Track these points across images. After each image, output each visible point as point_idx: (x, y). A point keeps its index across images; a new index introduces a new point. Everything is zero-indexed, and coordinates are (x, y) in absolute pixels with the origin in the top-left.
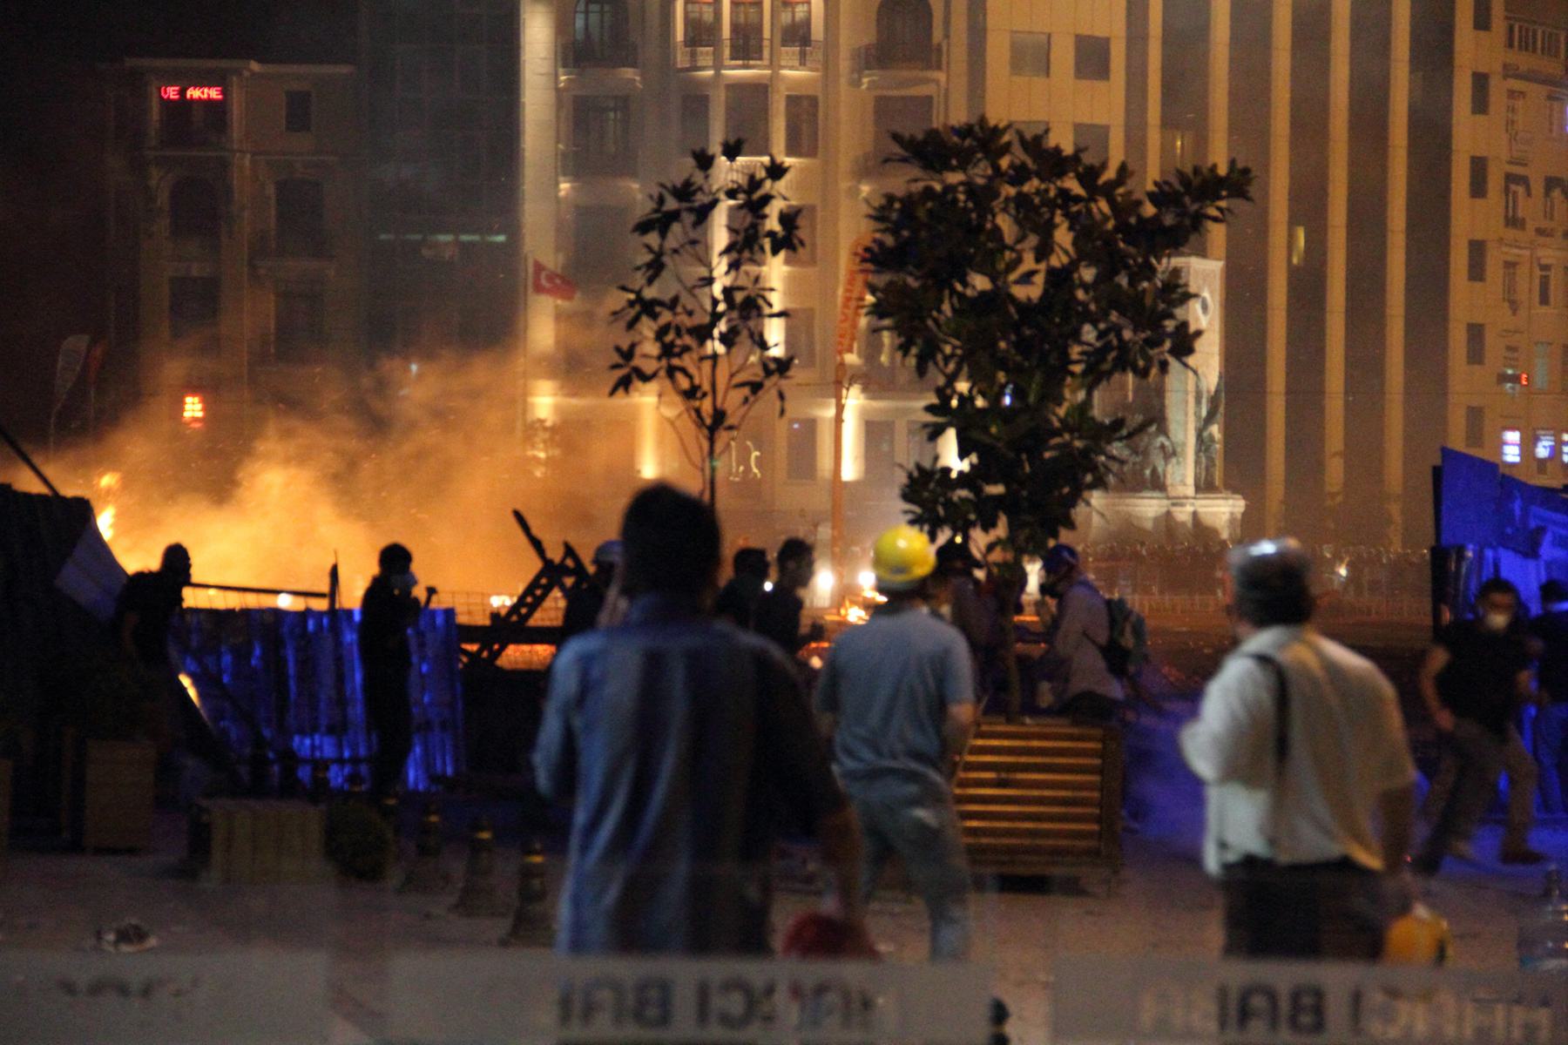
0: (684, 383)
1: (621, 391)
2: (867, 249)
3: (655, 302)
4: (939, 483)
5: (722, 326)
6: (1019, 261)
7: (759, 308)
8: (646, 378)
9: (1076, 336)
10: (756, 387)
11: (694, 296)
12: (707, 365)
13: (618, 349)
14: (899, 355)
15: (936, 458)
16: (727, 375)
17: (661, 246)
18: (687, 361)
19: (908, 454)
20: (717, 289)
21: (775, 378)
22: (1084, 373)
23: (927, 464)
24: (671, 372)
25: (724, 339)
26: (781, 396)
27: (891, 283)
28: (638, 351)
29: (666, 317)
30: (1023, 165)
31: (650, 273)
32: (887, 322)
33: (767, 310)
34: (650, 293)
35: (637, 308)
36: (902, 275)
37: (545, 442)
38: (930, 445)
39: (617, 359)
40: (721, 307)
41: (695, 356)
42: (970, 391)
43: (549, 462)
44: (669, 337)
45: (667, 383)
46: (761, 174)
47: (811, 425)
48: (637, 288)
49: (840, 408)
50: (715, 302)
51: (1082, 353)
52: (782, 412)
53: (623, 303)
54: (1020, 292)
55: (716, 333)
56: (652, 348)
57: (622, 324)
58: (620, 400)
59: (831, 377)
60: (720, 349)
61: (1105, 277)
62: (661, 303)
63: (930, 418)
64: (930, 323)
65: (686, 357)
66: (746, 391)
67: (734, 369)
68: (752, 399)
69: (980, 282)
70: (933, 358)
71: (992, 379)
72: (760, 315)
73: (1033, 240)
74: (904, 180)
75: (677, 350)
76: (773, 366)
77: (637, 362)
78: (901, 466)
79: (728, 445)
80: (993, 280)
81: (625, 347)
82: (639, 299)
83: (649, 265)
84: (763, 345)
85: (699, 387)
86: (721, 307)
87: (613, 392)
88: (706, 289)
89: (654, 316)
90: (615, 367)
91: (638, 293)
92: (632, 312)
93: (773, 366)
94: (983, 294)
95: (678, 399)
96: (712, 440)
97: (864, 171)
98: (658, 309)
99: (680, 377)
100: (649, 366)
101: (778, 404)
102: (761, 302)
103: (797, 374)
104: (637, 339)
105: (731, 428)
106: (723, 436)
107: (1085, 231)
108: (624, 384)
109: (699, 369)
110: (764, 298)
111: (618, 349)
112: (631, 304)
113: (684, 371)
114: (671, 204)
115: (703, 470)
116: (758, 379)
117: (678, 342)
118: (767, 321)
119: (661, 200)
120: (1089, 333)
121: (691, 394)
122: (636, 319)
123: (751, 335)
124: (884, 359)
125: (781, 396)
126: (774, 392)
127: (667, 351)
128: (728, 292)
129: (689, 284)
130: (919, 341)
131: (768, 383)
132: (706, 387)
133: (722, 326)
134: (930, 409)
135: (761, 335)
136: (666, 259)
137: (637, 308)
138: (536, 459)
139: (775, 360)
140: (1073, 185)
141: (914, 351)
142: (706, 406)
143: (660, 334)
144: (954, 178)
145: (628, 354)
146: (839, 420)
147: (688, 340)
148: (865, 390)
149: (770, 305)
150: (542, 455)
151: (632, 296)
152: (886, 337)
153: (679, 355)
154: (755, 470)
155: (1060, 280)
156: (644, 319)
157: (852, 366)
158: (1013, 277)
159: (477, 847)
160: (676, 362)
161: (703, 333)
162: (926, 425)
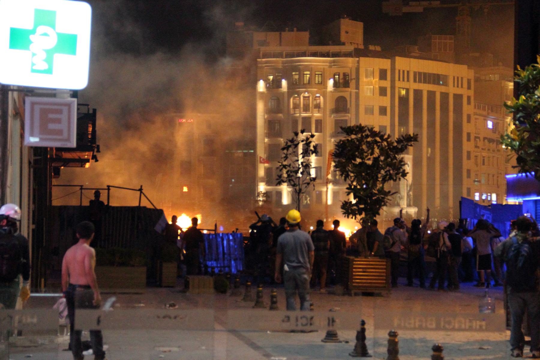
5: (301, 170)
9: (379, 173)
10: (308, 184)
15: (349, 200)
18: (293, 178)
20: (300, 162)
23: (347, 201)
25: (302, 173)
26: (314, 186)
32: (338, 169)
40: (300, 166)
43: (263, 201)
44: (289, 173)
46: (309, 137)
49: (327, 188)
50: (299, 165)
55: (299, 172)
56: (285, 175)
58: (279, 187)
61: (385, 159)
63: (347, 191)
66: (306, 185)
69: (358, 160)
71: (362, 182)
72: (309, 168)
77: (282, 178)
83: (284, 157)
84: (310, 175)
96: (299, 195)
97: (332, 136)
100: (285, 180)
103: (317, 181)
105: (303, 193)
106: (301, 195)
107: (382, 150)
108: (279, 183)
113: (292, 180)
121: (294, 185)
124: (337, 177)
125: (314, 186)
127: (289, 176)
128: (302, 163)
131: (311, 183)
132: (297, 184)
133: (301, 170)
134: (347, 188)
135: (310, 172)
136: (288, 156)
138: (260, 200)
139: (313, 178)
140: (378, 139)
141: (344, 175)
142: (297, 188)
147: (294, 174)
148: (333, 184)
152: (338, 173)
156: (284, 169)
159: (247, 286)
161: (297, 172)
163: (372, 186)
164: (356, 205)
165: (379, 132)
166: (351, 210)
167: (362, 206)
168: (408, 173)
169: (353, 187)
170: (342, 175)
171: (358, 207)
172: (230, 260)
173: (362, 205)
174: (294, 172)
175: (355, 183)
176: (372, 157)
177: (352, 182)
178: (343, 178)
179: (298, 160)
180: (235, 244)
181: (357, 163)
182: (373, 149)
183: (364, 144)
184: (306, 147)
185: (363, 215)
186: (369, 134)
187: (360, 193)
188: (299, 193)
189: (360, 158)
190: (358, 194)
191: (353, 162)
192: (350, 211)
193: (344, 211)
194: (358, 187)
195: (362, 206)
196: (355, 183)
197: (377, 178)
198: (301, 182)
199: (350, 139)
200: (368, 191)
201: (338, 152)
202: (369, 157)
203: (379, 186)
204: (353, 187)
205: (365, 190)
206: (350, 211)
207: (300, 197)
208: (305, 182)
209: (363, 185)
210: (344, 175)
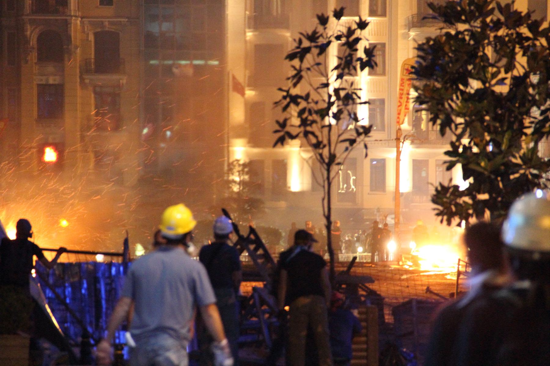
0: (314, 141)
1: (279, 144)
2: (413, 67)
3: (297, 97)
4: (453, 194)
5: (334, 109)
6: (499, 72)
7: (353, 99)
8: (293, 137)
9: (528, 113)
11: (319, 93)
12: (326, 130)
13: (278, 122)
14: (431, 124)
15: (451, 180)
16: (337, 136)
17: (300, 67)
18: (314, 128)
19: (436, 177)
20: (331, 90)
21: (362, 137)
22: (533, 134)
23: (446, 184)
25: (336, 116)
26: (366, 147)
27: (426, 86)
28: (288, 123)
29: (303, 104)
30: (499, 20)
31: (295, 81)
32: (424, 106)
33: (358, 101)
34: (294, 92)
35: (288, 100)
36: (432, 81)
37: (239, 171)
38: (449, 172)
39: (277, 127)
40: (333, 99)
41: (319, 125)
42: (470, 143)
44: (304, 116)
45: (304, 140)
46: (354, 26)
49: (399, 153)
51: (532, 123)
52: (366, 155)
53: (280, 97)
54: (498, 89)
55: (331, 114)
56: (296, 121)
57: (280, 108)
58: (280, 150)
59: (394, 136)
60: (333, 122)
62: (301, 97)
63: (448, 158)
64: (447, 106)
65: (314, 125)
66: (347, 144)
67: (341, 132)
68: (350, 148)
69: (475, 85)
72: (354, 103)
73: (504, 61)
74: (435, 30)
75: (309, 122)
76: (361, 130)
78: (432, 184)
79: (338, 173)
81: (281, 121)
82: (288, 95)
83: (294, 77)
84: (356, 119)
85: (322, 142)
87: (275, 145)
88: (326, 89)
89: (297, 104)
90: (276, 132)
91: (288, 92)
92: (285, 102)
93: (361, 130)
94: (477, 91)
95: (310, 148)
96: (329, 171)
98: (299, 100)
99: (311, 137)
100: (294, 131)
101: (364, 150)
102: (354, 96)
104: (288, 116)
105: (339, 164)
106: (334, 168)
108: (281, 141)
109: (322, 132)
110: (356, 94)
111: (278, 122)
112: (285, 98)
113: (313, 133)
114: (306, 44)
115: (324, 187)
116: (353, 138)
117: (310, 118)
118: (359, 106)
119: (300, 42)
120: (535, 112)
121: (317, 146)
122: (287, 106)
123: (350, 115)
124: (423, 126)
125: (366, 147)
126: (362, 145)
127: (304, 123)
128: (337, 91)
131: (358, 140)
132: (325, 142)
133: (334, 109)
134: (447, 153)
135: (355, 114)
136: (303, 73)
137: (288, 100)
139: (363, 127)
140: (525, 31)
141: (439, 122)
142: (326, 152)
143: (301, 113)
144: (462, 27)
145: (283, 125)
146: (398, 159)
147: (315, 117)
148: (412, 142)
149: (359, 98)
150: (237, 179)
151: (285, 94)
152: (424, 115)
153: (311, 125)
154: (353, 187)
155: (519, 83)
156: (292, 106)
158: (494, 82)
160: (309, 128)
161: (324, 113)
162: (445, 162)
163: (510, 146)
164: (469, 192)
165: (528, 15)
166: (457, 205)
167: (484, 197)
169: (461, 150)
170: (433, 121)
171: (474, 198)
173: (484, 193)
174: (317, 112)
175: (465, 141)
176: (509, 75)
177: (460, 137)
179: (327, 85)
181: (472, 91)
182: (512, 56)
183: (489, 44)
184: (348, 51)
186: (502, 19)
187: (479, 164)
188: (329, 165)
189: (478, 79)
190: (473, 166)
191: (461, 87)
192: (454, 209)
193: (441, 208)
194: (475, 150)
195: (484, 197)
196: (465, 141)
197: (522, 126)
198: (334, 138)
199: (453, 32)
200: (499, 159)
201: (424, 64)
202: (502, 75)
203: (526, 145)
204: (461, 150)
205: (489, 157)
206: (454, 209)
207: (332, 174)
209: (487, 144)
210: (439, 122)
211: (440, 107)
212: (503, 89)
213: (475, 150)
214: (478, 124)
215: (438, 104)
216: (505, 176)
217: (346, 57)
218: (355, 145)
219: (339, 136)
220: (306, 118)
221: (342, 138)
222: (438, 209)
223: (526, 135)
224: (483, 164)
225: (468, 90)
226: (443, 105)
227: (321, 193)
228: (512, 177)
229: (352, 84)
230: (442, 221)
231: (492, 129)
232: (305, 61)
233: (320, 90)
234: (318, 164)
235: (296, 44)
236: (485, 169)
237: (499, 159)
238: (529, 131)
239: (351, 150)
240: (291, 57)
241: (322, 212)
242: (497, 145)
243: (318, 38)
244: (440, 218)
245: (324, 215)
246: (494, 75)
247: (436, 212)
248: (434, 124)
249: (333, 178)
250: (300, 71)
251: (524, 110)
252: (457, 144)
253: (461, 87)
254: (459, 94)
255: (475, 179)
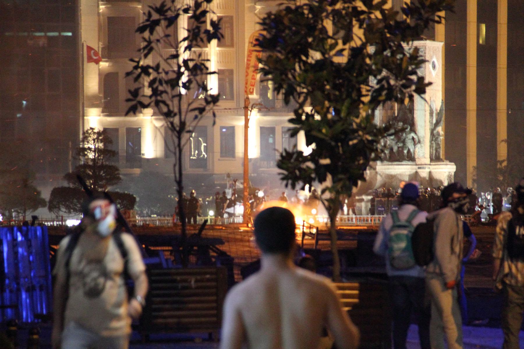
0: (165, 110)
1: (131, 113)
3: (148, 67)
4: (297, 160)
5: (184, 79)
6: (336, 44)
8: (145, 106)
9: (366, 82)
12: (176, 101)
13: (130, 91)
15: (295, 146)
18: (164, 97)
19: (282, 144)
21: (211, 105)
22: (371, 102)
24: (157, 103)
25: (185, 86)
26: (214, 115)
27: (270, 57)
28: (141, 93)
31: (146, 52)
32: (270, 76)
38: (293, 140)
39: (130, 96)
40: (183, 69)
41: (170, 96)
44: (155, 86)
45: (156, 109)
47: (232, 130)
48: (137, 60)
54: (337, 60)
58: (132, 119)
59: (242, 105)
60: (183, 91)
62: (152, 68)
63: (291, 126)
64: (290, 76)
65: (164, 95)
66: (196, 113)
67: (190, 101)
68: (199, 116)
69: (316, 56)
70: (293, 94)
73: (342, 33)
78: (277, 150)
80: (323, 54)
83: (144, 48)
84: (205, 88)
85: (172, 112)
86: (183, 69)
87: (127, 114)
88: (175, 61)
89: (148, 74)
90: (128, 100)
93: (209, 99)
94: (317, 61)
96: (179, 138)
99: (162, 105)
100: (146, 101)
101: (212, 118)
102: (203, 67)
103: (221, 104)
105: (190, 132)
106: (185, 136)
109: (172, 101)
110: (203, 64)
111: (130, 91)
113: (164, 102)
114: (155, 16)
115: (175, 154)
119: (150, 15)
120: (373, 81)
121: (168, 114)
122: (139, 76)
126: (210, 114)
127: (155, 92)
128: (185, 62)
129: (165, 58)
130: (285, 86)
131: (207, 108)
132: (176, 110)
134: (291, 121)
136: (153, 45)
139: (212, 96)
141: (283, 91)
142: (176, 120)
143: (151, 84)
145: (135, 93)
146: (246, 127)
148: (260, 111)
155: (357, 53)
157: (253, 99)
158: (333, 52)
160: (159, 98)
161: (174, 83)
162: (289, 130)
163: (349, 114)
166: (300, 170)
167: (326, 161)
168: (430, 84)
169: (304, 117)
170: (277, 89)
171: (316, 163)
172: (19, 290)
173: (325, 158)
174: (167, 82)
175: (308, 109)
176: (347, 46)
177: (302, 105)
178: (281, 96)
179: (176, 56)
180: (30, 253)
181: (313, 62)
184: (196, 24)
185: (328, 183)
187: (320, 131)
190: (314, 133)
191: (304, 58)
192: (297, 172)
193: (285, 172)
194: (318, 117)
195: (326, 161)
197: (360, 95)
198: (184, 107)
202: (340, 46)
204: (304, 117)
206: (297, 172)
207: (183, 141)
208: (195, 105)
210: (283, 91)
211: (284, 77)
212: (342, 60)
213: (318, 117)
214: (319, 94)
215: (281, 74)
216: (345, 142)
217: (194, 30)
218: (204, 113)
219: (189, 105)
220: (157, 87)
221: (192, 107)
222: (283, 174)
223: (363, 103)
224: (324, 131)
225: (310, 60)
226: (286, 75)
227: (173, 160)
228: (351, 143)
229: (200, 55)
230: (286, 186)
231: (332, 97)
232: (155, 33)
233: (170, 61)
234: (170, 132)
235: (146, 18)
236: (326, 135)
237: (339, 127)
238: (366, 99)
239: (201, 117)
240: (141, 30)
241: (174, 178)
242: (338, 112)
243: (166, 11)
244: (285, 182)
245: (176, 181)
246: (333, 46)
247: (281, 176)
248: (278, 93)
249: (184, 145)
250: (150, 42)
251: (361, 79)
252: (300, 111)
253: (304, 58)
254: (302, 65)
255: (317, 145)
